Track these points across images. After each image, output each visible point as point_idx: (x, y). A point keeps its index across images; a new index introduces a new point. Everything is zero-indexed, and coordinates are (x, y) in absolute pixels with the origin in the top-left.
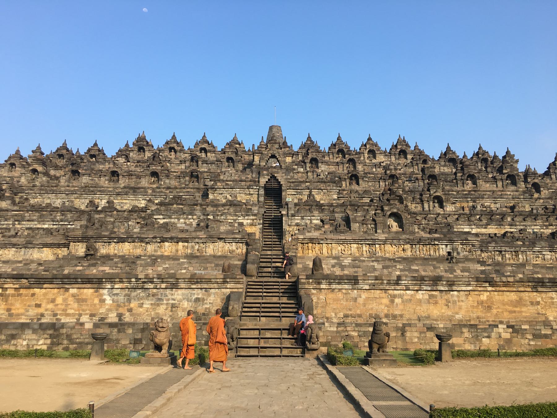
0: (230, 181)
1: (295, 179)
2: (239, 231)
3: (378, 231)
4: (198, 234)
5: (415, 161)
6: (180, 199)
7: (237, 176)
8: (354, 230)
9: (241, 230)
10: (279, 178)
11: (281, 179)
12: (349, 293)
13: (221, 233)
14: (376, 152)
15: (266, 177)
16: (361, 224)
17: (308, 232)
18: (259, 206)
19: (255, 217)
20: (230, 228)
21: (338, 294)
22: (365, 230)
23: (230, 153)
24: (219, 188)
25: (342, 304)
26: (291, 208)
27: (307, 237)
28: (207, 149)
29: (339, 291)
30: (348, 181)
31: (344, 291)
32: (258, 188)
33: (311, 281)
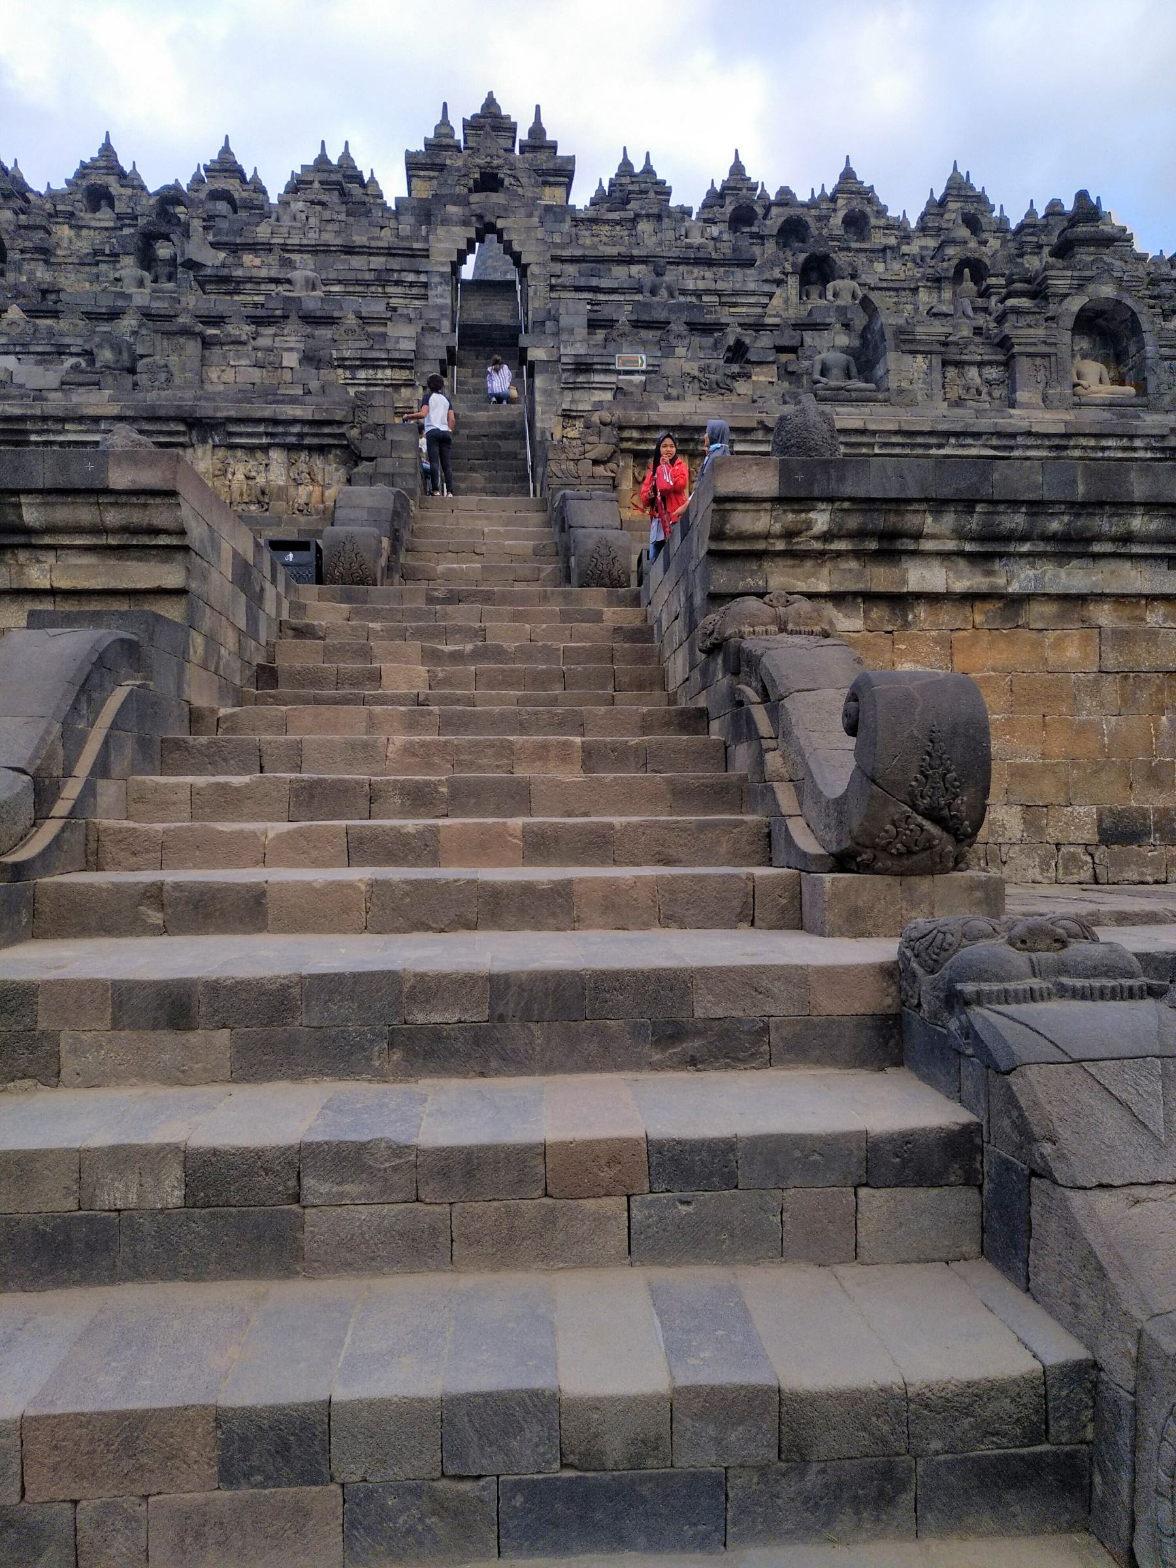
0: (301, 249)
1: (583, 246)
2: (308, 392)
3: (1021, 396)
4: (75, 399)
5: (1031, 234)
6: (53, 297)
7: (330, 227)
8: (901, 391)
9: (314, 385)
10: (513, 237)
11: (522, 243)
12: (1152, 636)
13: (210, 398)
14: (873, 221)
15: (456, 229)
16: (936, 361)
17: (668, 398)
18: (421, 323)
19: (404, 375)
20: (256, 375)
21: (1057, 645)
22: (953, 395)
23: (316, 185)
24: (250, 280)
25: (1082, 729)
26: (571, 331)
27: (666, 416)
28: (236, 196)
29: (1062, 617)
30: (793, 282)
31: (1105, 616)
32: (423, 278)
33: (821, 520)
